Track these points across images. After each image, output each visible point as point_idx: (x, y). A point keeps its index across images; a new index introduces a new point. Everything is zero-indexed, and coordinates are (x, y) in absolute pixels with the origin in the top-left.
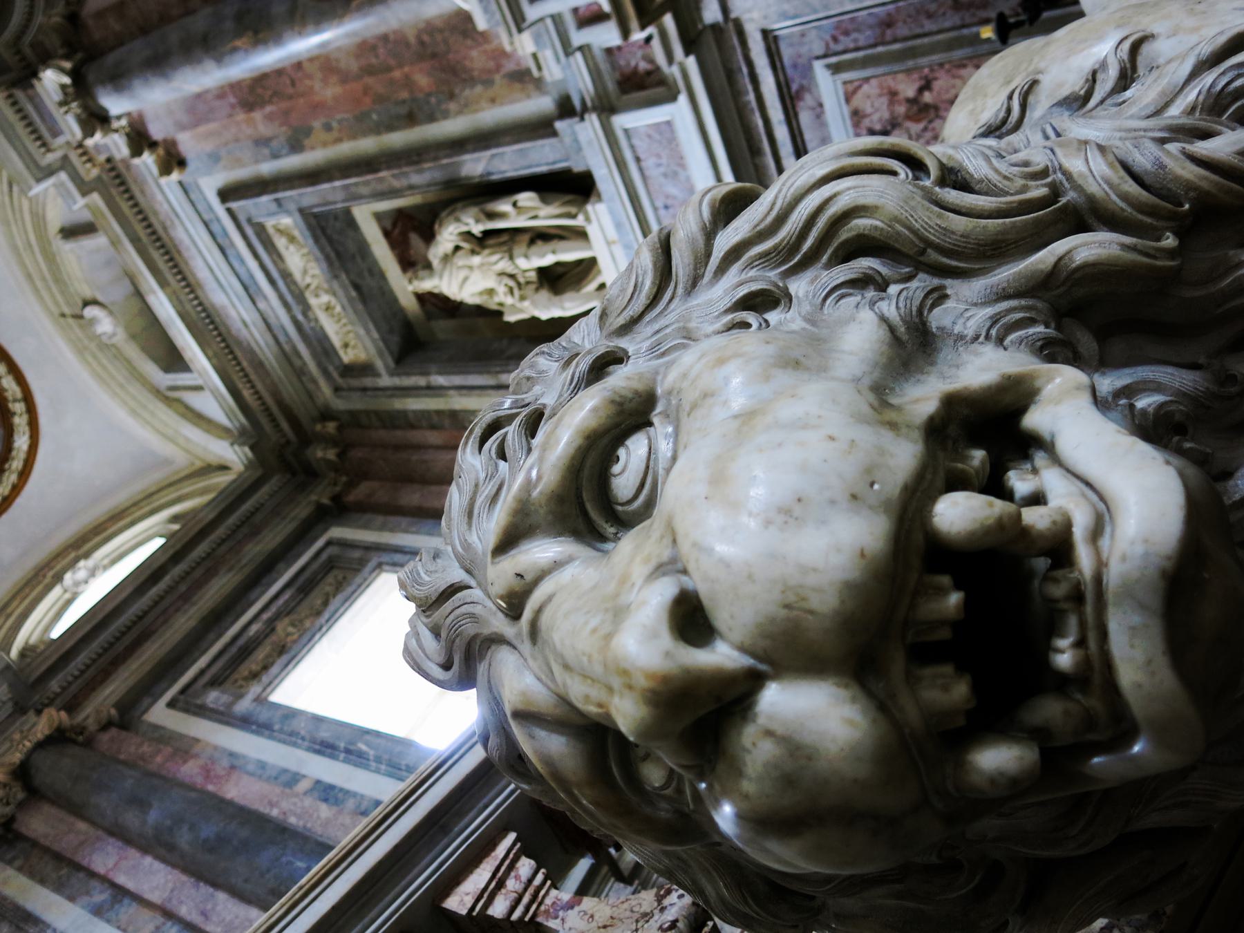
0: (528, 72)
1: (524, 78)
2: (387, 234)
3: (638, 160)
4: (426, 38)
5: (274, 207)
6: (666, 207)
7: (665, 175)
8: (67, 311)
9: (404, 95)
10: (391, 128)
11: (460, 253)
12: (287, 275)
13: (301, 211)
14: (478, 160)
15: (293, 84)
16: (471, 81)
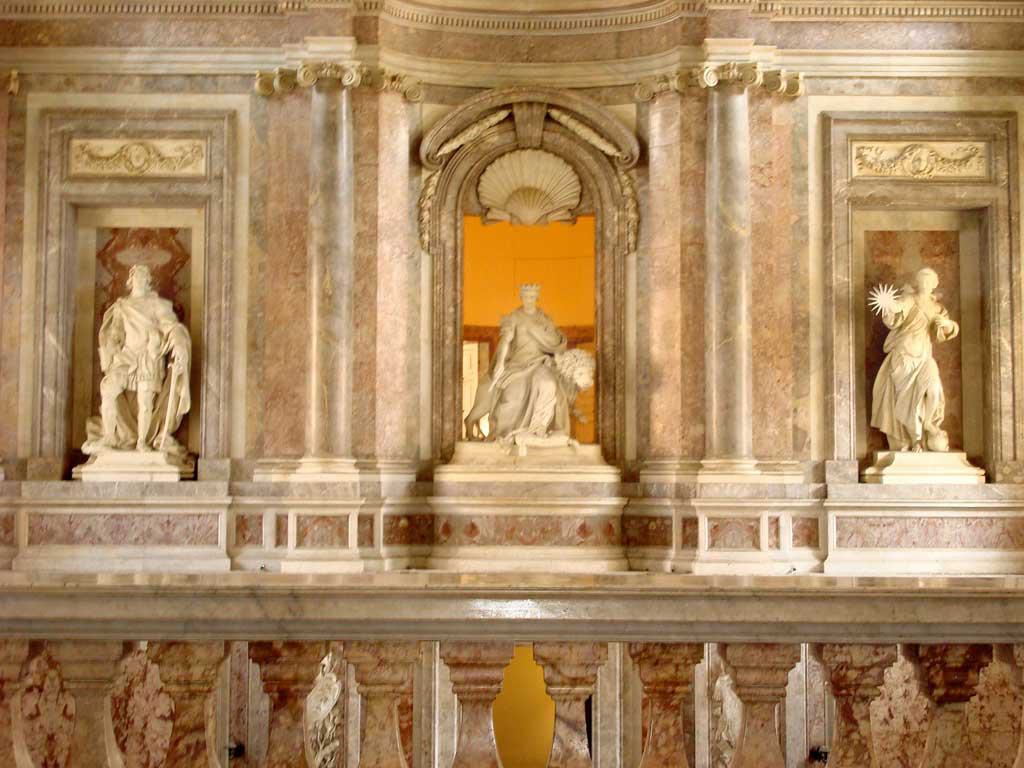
2: (173, 231)
3: (199, 516)
4: (296, 401)
5: (216, 170)
6: (168, 522)
7: (188, 529)
9: (268, 351)
10: (250, 324)
11: (157, 337)
12: (161, 135)
14: (218, 384)
15: (296, 275)
16: (265, 407)
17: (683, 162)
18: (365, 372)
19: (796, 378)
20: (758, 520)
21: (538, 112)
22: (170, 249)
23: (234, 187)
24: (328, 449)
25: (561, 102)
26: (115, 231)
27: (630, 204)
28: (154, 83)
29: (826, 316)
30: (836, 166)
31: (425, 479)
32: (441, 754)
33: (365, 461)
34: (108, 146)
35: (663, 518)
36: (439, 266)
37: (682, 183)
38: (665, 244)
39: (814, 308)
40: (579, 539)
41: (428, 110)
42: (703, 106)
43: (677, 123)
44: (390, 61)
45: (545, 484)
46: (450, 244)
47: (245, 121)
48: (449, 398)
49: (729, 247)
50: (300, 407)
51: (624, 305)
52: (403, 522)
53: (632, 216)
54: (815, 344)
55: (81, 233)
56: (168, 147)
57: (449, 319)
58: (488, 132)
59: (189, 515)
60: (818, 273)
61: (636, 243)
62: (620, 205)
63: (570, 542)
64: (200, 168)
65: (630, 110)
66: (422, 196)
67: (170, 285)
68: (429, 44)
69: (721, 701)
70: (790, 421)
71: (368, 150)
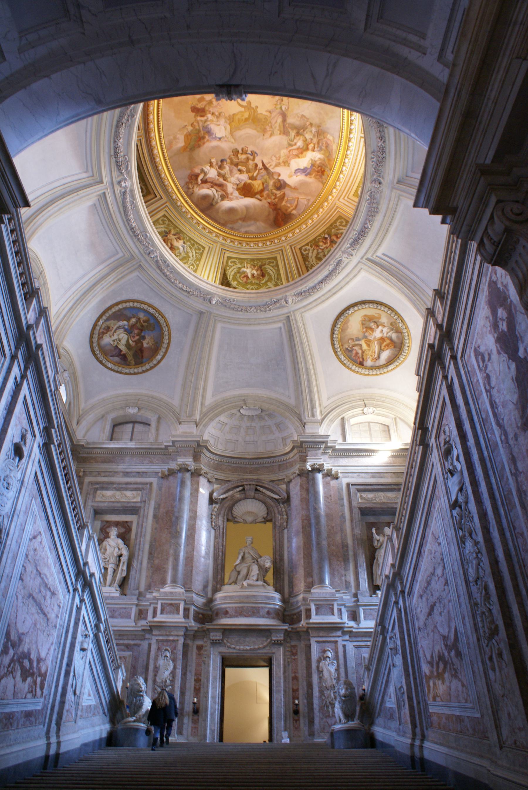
0: (150, 589)
1: (149, 588)
2: (127, 522)
5: (144, 499)
8: (140, 402)
9: (155, 555)
10: (150, 546)
12: (126, 489)
13: (140, 507)
14: (137, 566)
16: (153, 574)
17: (301, 495)
18: (190, 559)
19: (345, 564)
20: (333, 605)
21: (253, 487)
22: (125, 527)
23: (149, 504)
24: (174, 581)
25: (261, 484)
26: (107, 522)
27: (284, 513)
28: (126, 474)
29: (354, 544)
30: (353, 498)
31: (211, 601)
32: (212, 697)
33: (188, 590)
34: (109, 493)
35: (298, 613)
36: (217, 533)
37: (301, 501)
38: (296, 523)
39: (350, 541)
40: (266, 616)
41: (216, 486)
42: (308, 476)
43: (299, 484)
44: (205, 469)
45: (254, 596)
46: (221, 526)
47: (155, 486)
48: (219, 577)
49: (318, 517)
50: (166, 572)
51: (283, 545)
52: (201, 616)
53: (285, 517)
54: (351, 553)
55: (96, 522)
56: (129, 493)
57: (220, 550)
58: (236, 493)
59: (121, 608)
60: (350, 531)
61: (287, 525)
62: (280, 514)
63: (263, 617)
64: (138, 499)
65: (284, 486)
66: (213, 511)
67: (124, 536)
68: (217, 467)
69: (322, 671)
70: (343, 578)
71: (195, 492)
